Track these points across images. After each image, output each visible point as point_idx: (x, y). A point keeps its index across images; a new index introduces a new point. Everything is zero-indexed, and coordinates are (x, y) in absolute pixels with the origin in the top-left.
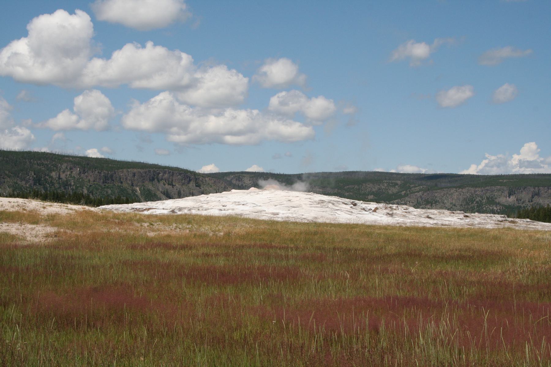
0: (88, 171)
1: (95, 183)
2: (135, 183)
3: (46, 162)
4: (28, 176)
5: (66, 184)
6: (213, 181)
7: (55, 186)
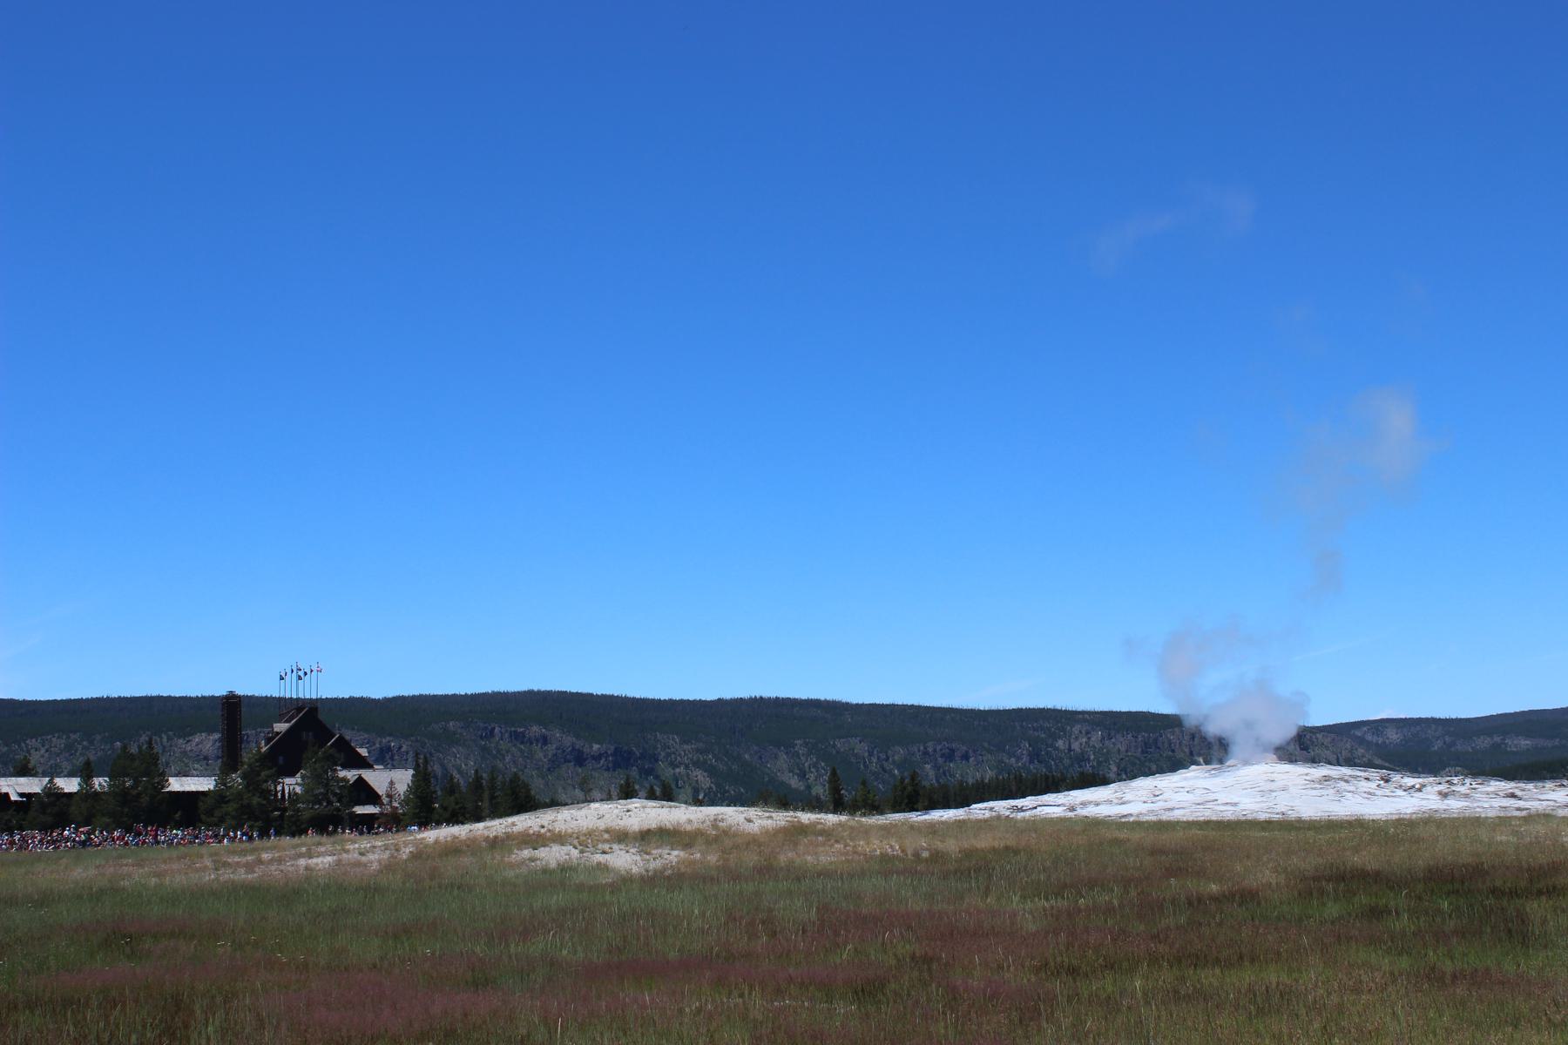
0: (1115, 736)
1: (1129, 754)
5: (1081, 758)
6: (1329, 739)
7: (1063, 764)
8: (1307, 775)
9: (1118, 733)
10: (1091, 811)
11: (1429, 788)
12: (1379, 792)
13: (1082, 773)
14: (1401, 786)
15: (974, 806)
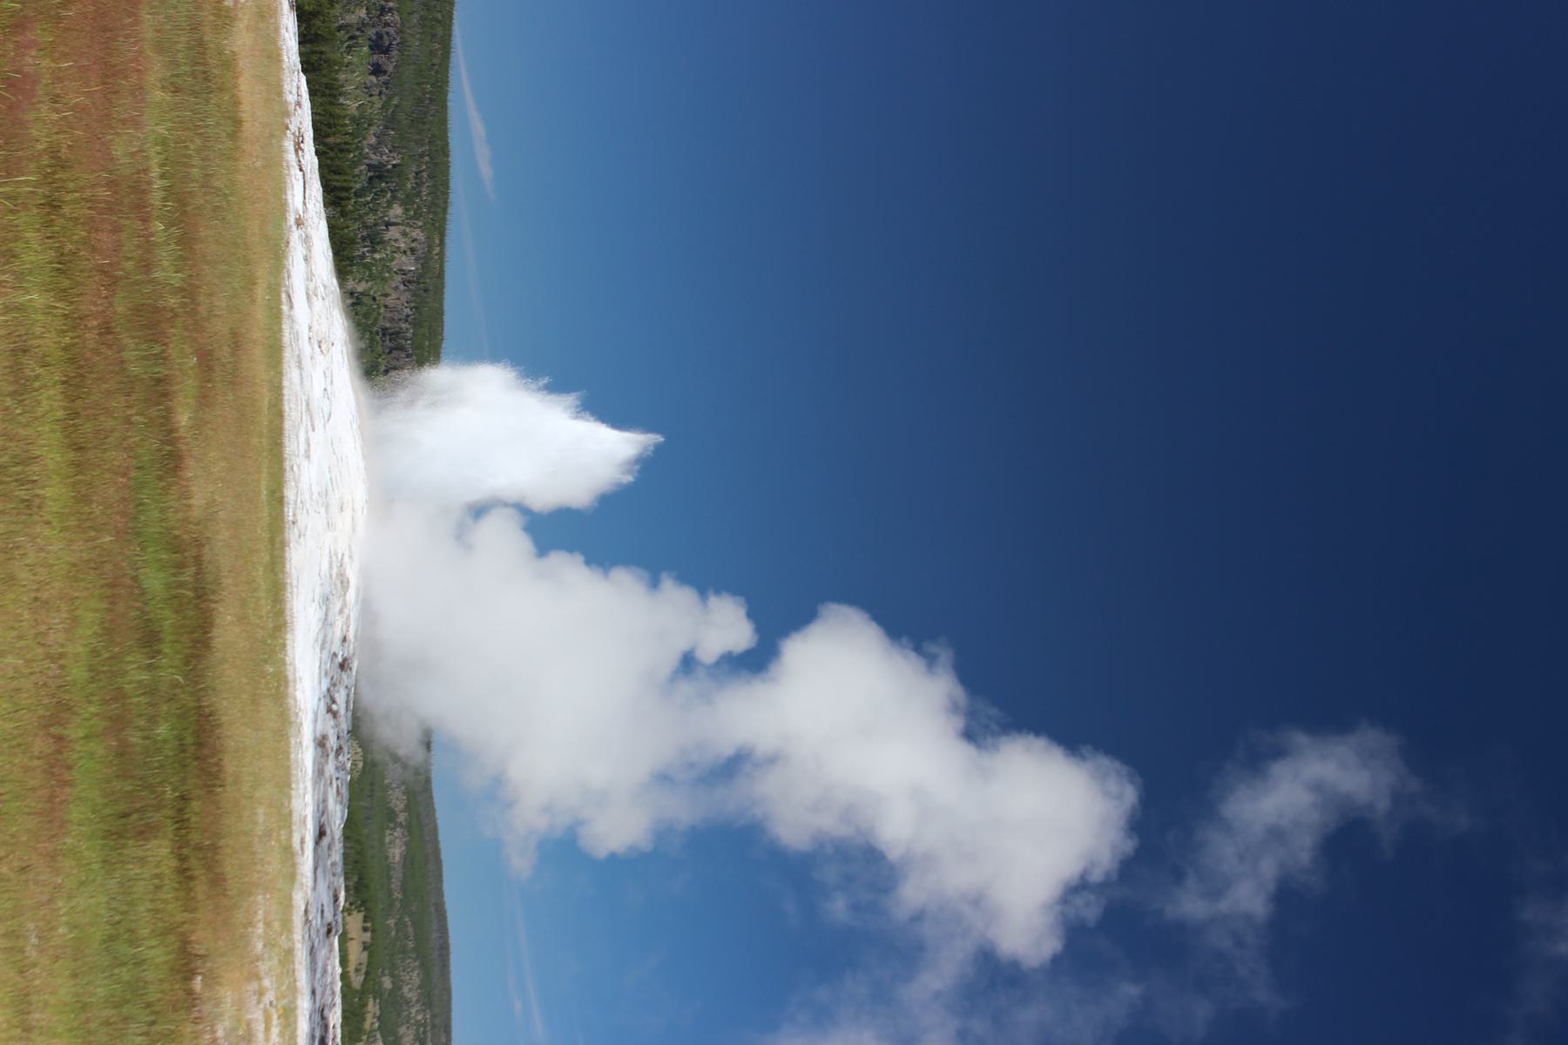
0: (409, 290)
1: (382, 310)
3: (425, 191)
4: (390, 151)
5: (375, 241)
7: (368, 214)
8: (351, 557)
9: (414, 295)
10: (296, 251)
11: (332, 723)
12: (325, 655)
13: (353, 241)
14: (334, 685)
15: (303, 78)
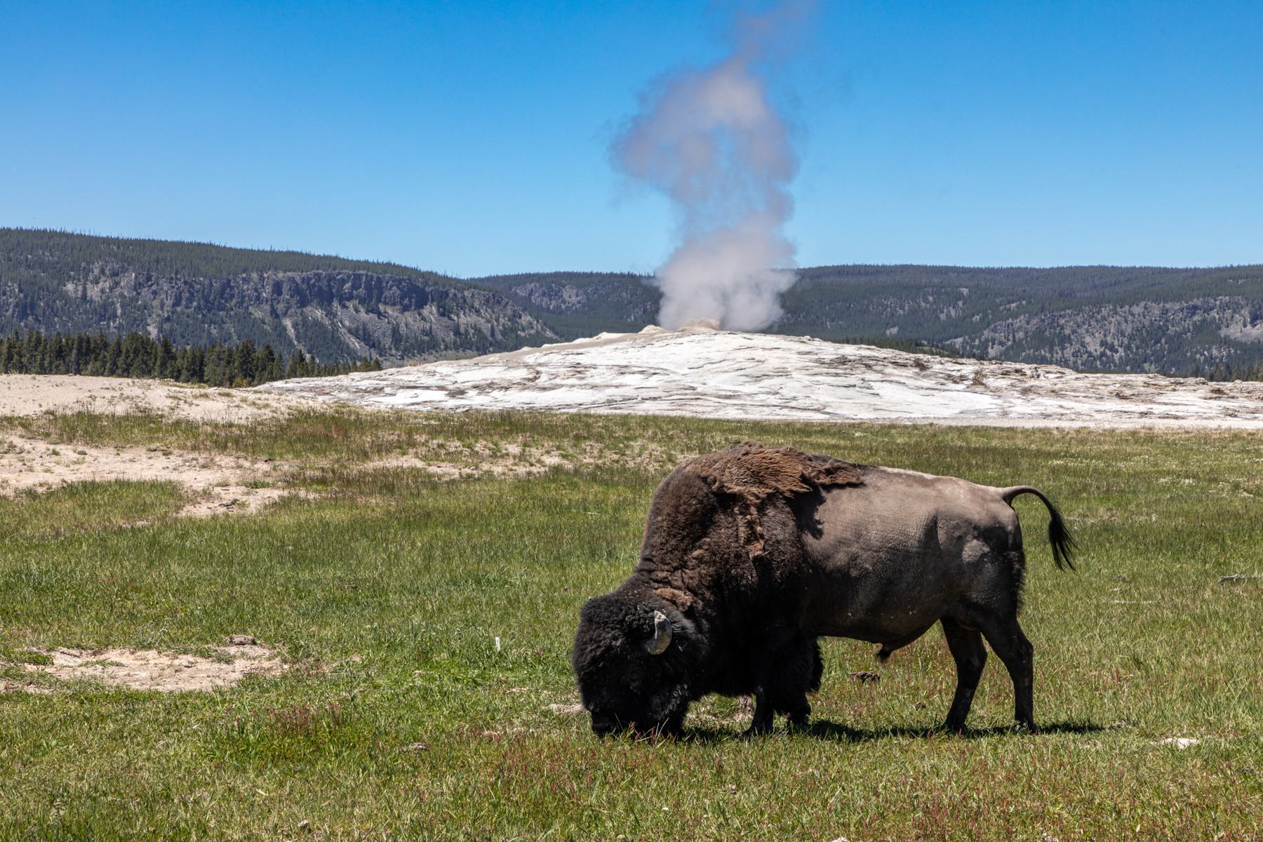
2: (280, 307)
